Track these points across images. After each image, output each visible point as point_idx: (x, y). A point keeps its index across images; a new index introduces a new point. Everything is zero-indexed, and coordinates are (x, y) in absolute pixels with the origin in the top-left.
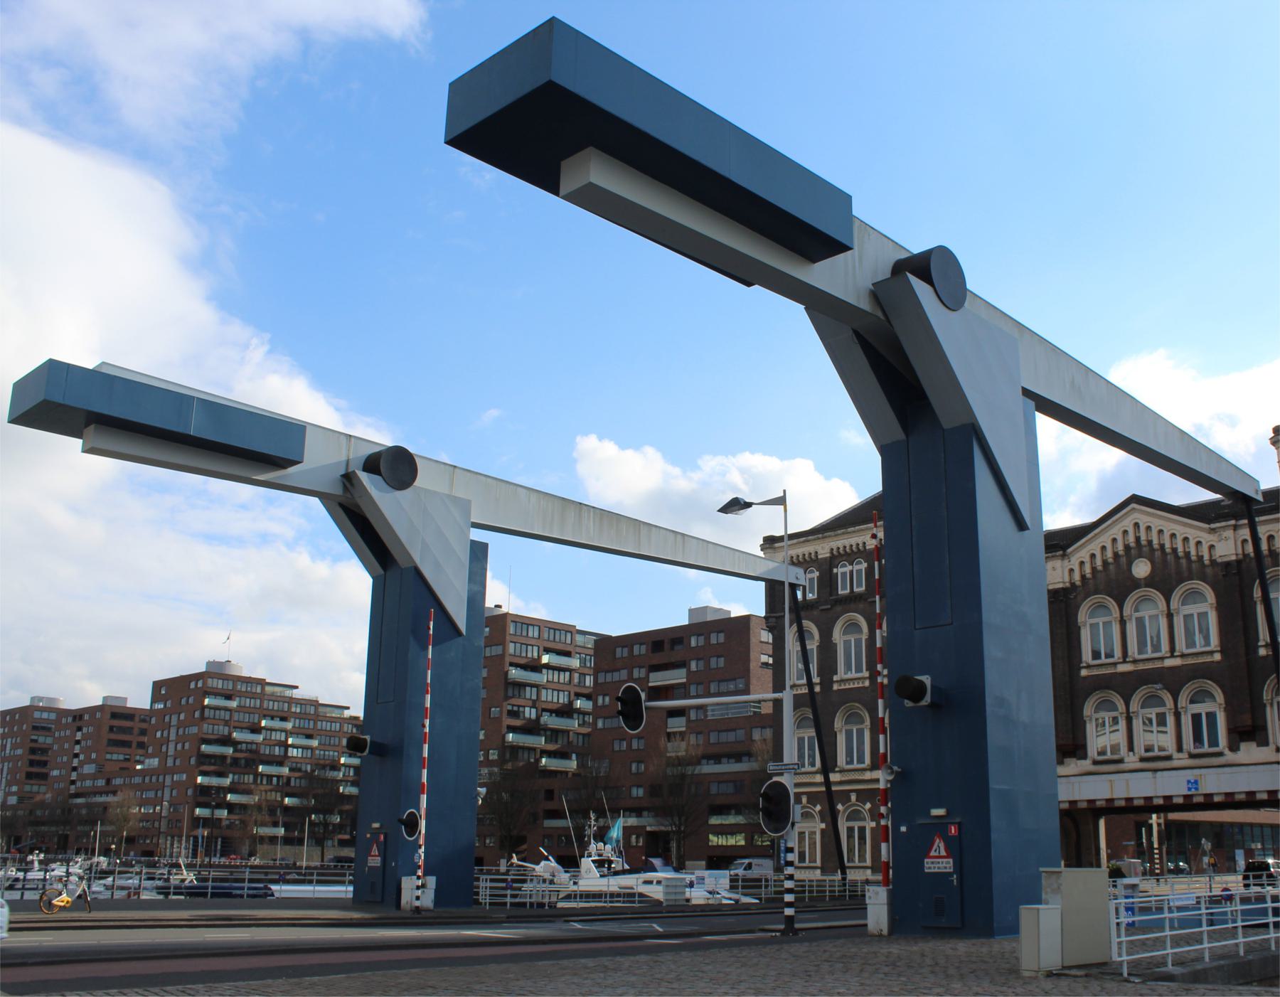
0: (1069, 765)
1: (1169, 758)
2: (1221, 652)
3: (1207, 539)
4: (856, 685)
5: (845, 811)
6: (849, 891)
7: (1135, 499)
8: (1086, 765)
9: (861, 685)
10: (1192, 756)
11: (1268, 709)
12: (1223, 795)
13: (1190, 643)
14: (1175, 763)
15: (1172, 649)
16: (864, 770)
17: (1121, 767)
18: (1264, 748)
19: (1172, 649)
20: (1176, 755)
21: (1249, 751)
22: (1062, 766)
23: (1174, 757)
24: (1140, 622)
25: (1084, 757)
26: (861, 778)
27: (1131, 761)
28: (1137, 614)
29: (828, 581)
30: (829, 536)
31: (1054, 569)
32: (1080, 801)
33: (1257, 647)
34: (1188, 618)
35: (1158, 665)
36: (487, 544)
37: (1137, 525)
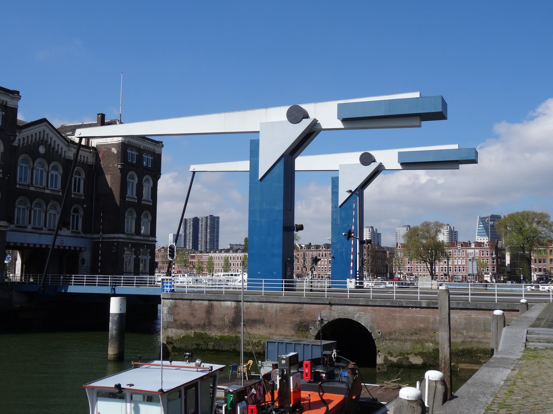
1: (41, 229)
3: (65, 148)
6: (51, 281)
7: (44, 120)
10: (49, 230)
13: (52, 186)
14: (43, 232)
17: (25, 229)
20: (44, 228)
25: (13, 223)
27: (29, 229)
34: (52, 175)
37: (44, 131)
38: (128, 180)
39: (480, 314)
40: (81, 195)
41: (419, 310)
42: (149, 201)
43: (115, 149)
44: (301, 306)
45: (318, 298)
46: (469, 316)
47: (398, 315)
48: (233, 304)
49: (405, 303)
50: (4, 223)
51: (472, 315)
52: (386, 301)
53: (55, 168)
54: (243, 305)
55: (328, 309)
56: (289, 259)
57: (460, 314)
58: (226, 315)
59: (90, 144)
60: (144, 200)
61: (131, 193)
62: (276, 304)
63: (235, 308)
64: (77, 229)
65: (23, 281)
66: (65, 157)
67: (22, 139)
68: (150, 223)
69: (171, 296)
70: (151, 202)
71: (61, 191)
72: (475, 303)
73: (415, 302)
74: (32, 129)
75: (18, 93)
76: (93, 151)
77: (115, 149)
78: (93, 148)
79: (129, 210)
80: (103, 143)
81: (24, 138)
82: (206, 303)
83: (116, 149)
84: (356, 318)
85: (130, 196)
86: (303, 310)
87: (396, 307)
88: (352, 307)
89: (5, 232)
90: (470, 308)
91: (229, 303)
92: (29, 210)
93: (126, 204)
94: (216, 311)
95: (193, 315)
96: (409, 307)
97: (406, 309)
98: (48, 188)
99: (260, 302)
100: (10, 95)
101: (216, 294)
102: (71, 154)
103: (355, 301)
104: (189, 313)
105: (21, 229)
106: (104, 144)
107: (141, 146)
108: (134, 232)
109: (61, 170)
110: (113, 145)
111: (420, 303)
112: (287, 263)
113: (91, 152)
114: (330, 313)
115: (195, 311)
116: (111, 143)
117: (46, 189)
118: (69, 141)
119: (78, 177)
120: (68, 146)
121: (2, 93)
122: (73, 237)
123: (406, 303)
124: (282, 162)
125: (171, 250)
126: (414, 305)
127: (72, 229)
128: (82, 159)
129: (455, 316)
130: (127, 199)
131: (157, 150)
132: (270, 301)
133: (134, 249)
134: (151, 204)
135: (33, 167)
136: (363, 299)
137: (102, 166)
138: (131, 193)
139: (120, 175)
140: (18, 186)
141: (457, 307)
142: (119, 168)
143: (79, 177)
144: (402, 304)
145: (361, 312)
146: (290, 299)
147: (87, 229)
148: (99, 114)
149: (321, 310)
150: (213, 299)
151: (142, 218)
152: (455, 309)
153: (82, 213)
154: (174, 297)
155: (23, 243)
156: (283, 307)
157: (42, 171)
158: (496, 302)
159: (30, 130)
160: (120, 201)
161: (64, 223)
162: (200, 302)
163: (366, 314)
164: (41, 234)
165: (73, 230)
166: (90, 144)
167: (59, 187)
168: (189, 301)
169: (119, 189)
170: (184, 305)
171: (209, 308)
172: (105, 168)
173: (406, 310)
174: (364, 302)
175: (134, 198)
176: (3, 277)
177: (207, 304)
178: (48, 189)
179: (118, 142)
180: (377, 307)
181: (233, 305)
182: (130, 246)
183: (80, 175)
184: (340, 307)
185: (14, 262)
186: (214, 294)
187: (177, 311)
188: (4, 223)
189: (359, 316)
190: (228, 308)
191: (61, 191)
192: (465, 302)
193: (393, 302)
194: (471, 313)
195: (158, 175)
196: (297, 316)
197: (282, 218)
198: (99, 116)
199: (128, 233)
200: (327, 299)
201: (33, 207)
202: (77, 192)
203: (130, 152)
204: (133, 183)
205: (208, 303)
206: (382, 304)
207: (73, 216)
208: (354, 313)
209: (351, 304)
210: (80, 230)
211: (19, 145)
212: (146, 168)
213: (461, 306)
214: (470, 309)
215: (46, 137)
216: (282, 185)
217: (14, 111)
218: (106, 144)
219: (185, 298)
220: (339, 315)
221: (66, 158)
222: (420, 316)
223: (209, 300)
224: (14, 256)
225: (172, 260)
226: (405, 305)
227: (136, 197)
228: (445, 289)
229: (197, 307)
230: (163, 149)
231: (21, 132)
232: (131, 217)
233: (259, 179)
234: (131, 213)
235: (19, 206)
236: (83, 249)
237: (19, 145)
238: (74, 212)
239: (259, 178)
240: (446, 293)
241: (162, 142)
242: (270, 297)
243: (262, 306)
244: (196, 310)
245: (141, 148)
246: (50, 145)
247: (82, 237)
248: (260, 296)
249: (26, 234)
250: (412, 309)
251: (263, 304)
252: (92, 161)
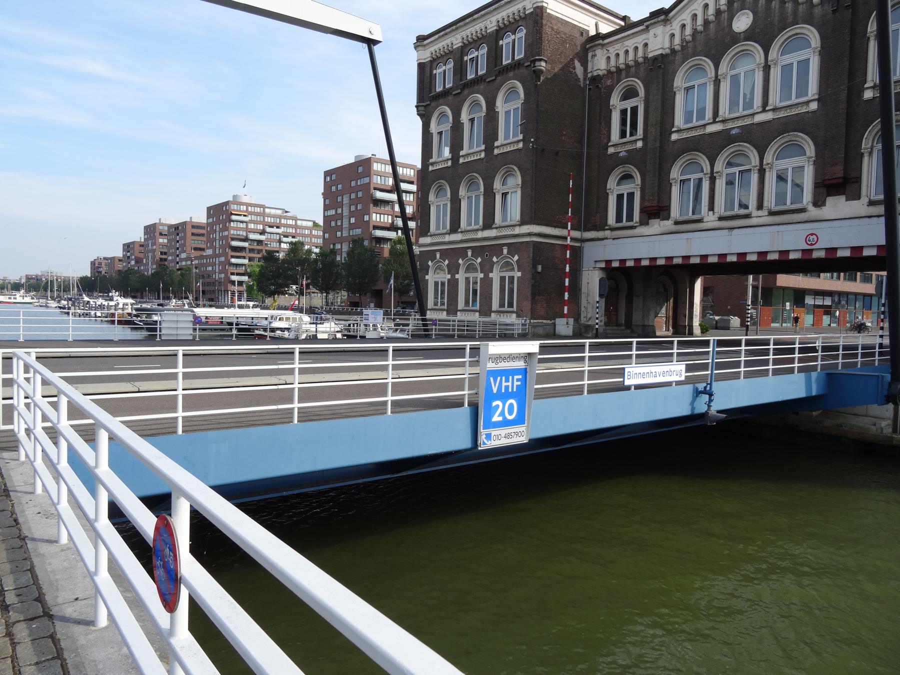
0: (654, 225)
2: (819, 100)
5: (464, 264)
8: (668, 224)
10: (772, 213)
11: (866, 159)
12: (801, 252)
14: (753, 221)
15: (765, 103)
16: (477, 230)
19: (765, 103)
20: (755, 213)
21: (837, 206)
22: (647, 226)
24: (735, 79)
25: (668, 217)
26: (475, 237)
28: (734, 72)
31: (655, 36)
33: (862, 90)
50: (528, 229)
188: (528, 229)
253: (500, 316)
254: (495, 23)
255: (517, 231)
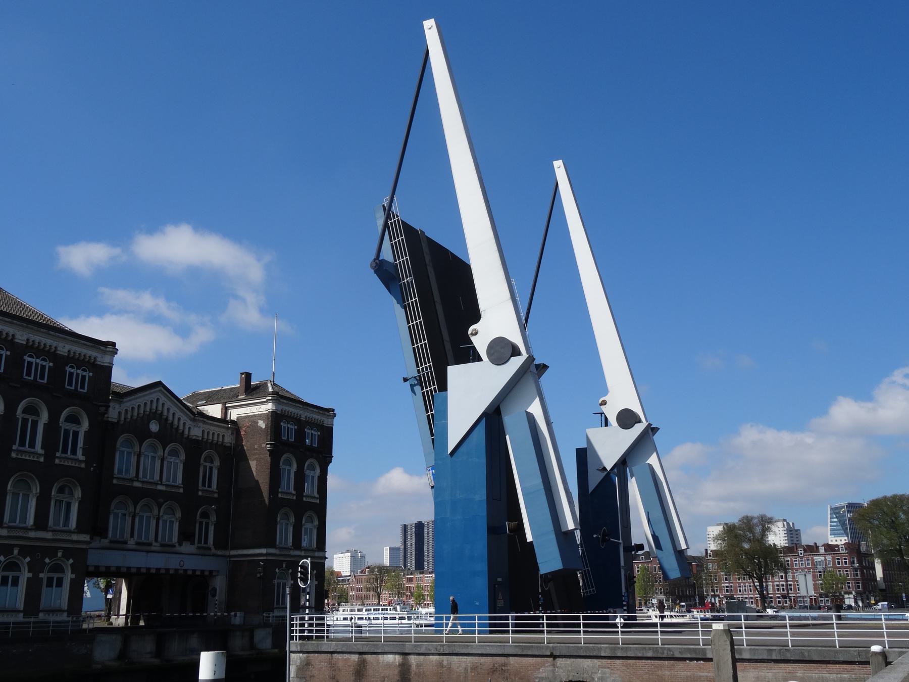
1: (150, 544)
3: (189, 423)
4: (31, 458)
5: (4, 562)
7: (159, 384)
8: (105, 542)
9: (35, 459)
10: (162, 545)
14: (153, 548)
18: (193, 546)
20: (154, 544)
21: (187, 548)
23: (153, 545)
25: (106, 538)
27: (131, 543)
29: (57, 374)
30: (32, 329)
32: (132, 567)
35: (153, 487)
36: (576, 449)
37: (158, 399)
38: (282, 466)
39: (811, 670)
40: (178, 487)
41: (703, 664)
42: (314, 497)
43: (262, 421)
44: (506, 661)
45: (532, 646)
46: (791, 674)
47: (667, 673)
48: (397, 658)
49: (678, 653)
51: (798, 673)
52: (645, 648)
53: (174, 453)
54: (413, 659)
55: (549, 664)
56: (499, 580)
57: (774, 671)
58: (386, 679)
59: (229, 417)
60: (306, 496)
61: (288, 485)
62: (465, 657)
63: (400, 665)
64: (206, 542)
65: (129, 625)
66: (189, 436)
67: (123, 412)
68: (316, 530)
69: (301, 647)
70: (317, 498)
71: (181, 487)
72: (799, 650)
73: (695, 650)
74: (140, 397)
75: (114, 344)
76: (232, 426)
77: (262, 421)
78: (233, 422)
79: (308, 515)
80: (247, 415)
81: (126, 411)
82: (355, 657)
83: (264, 422)
84: (596, 679)
85: (285, 490)
86: (509, 668)
87: (663, 660)
88: (589, 660)
89: (85, 551)
90: (792, 659)
91: (390, 658)
92: (131, 516)
93: (277, 503)
94: (370, 671)
95: (334, 678)
96: (684, 659)
97: (680, 662)
98: (138, 479)
99: (440, 654)
100: (102, 348)
101: (370, 643)
102: (196, 432)
103: (593, 649)
104: (329, 676)
105: (119, 545)
106: (247, 416)
107: (302, 416)
108: (291, 544)
109: (183, 457)
110: (259, 416)
111: (704, 651)
112: (497, 586)
113: (228, 428)
114: (553, 672)
115: (338, 672)
116: (257, 413)
117: (135, 480)
118: (196, 413)
119: (208, 465)
120: (194, 420)
121: (89, 346)
122: (202, 555)
123: (680, 652)
124: (482, 424)
125: (303, 570)
126: (694, 656)
127: (198, 543)
128: (216, 438)
129: (767, 674)
130: (280, 495)
131: (327, 422)
132: (454, 652)
133: (290, 571)
134: (318, 501)
135: (140, 452)
136: (607, 645)
137: (245, 448)
138: (288, 485)
139: (269, 459)
140: (115, 481)
141: (769, 658)
142: (268, 450)
143: (211, 465)
144: (673, 654)
145: (605, 669)
146: (488, 648)
147: (221, 543)
148: (242, 374)
149: (538, 667)
150: (366, 651)
151: (303, 522)
152: (766, 661)
153: (213, 518)
154: (305, 649)
155: (120, 567)
156: (476, 663)
157: (153, 458)
158: (838, 647)
159: (136, 398)
160: (270, 498)
161: (186, 535)
162: (345, 656)
163: (614, 673)
164: (148, 552)
165: (199, 545)
166: (229, 417)
167: (179, 480)
168: (329, 655)
169: (268, 480)
170: (320, 661)
171: (360, 666)
172: (248, 450)
173: (681, 664)
174: (608, 650)
175: (291, 494)
176: (79, 621)
177: (356, 660)
178: (161, 484)
179: (267, 412)
180: (631, 661)
181: (397, 660)
182: (284, 566)
183: (212, 462)
184: (569, 661)
185: (118, 596)
186: (368, 643)
187: (310, 673)
189: (602, 677)
190: (388, 666)
191: (182, 486)
192: (782, 648)
193: (656, 650)
194: (794, 668)
195: (328, 459)
196: (499, 677)
197: (485, 514)
198: (243, 376)
199: (281, 546)
200: (547, 647)
201: (137, 511)
202: (206, 488)
203: (309, 431)
204: (289, 471)
205: (359, 658)
206: (640, 655)
207: (201, 523)
208: (593, 671)
209: (588, 655)
210: (210, 544)
211: (119, 421)
212: (310, 449)
213: (776, 656)
214: (792, 660)
215: (160, 408)
216: (484, 461)
217: (107, 371)
218: (250, 416)
219: (323, 649)
220: (569, 676)
221: (190, 437)
222: (706, 676)
223: (360, 653)
224: (118, 587)
225: (304, 587)
226: (677, 655)
227: (294, 492)
228: (723, 629)
229: (340, 665)
230: (336, 420)
231: (121, 402)
232: (287, 522)
233: (449, 453)
234: (287, 516)
235: (116, 511)
236: (214, 574)
237: (119, 421)
238: (201, 517)
239: (449, 451)
240: (725, 637)
241: (334, 409)
242: (454, 645)
243: (443, 661)
244: (339, 670)
245: (302, 419)
246: (167, 419)
247: (214, 555)
248: (440, 643)
249: (125, 552)
250: (691, 663)
251: (445, 658)
252: (231, 440)
253: (49, 615)
254: (66, 350)
255: (75, 537)
